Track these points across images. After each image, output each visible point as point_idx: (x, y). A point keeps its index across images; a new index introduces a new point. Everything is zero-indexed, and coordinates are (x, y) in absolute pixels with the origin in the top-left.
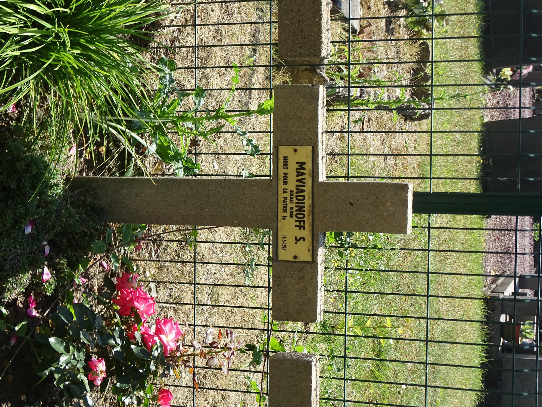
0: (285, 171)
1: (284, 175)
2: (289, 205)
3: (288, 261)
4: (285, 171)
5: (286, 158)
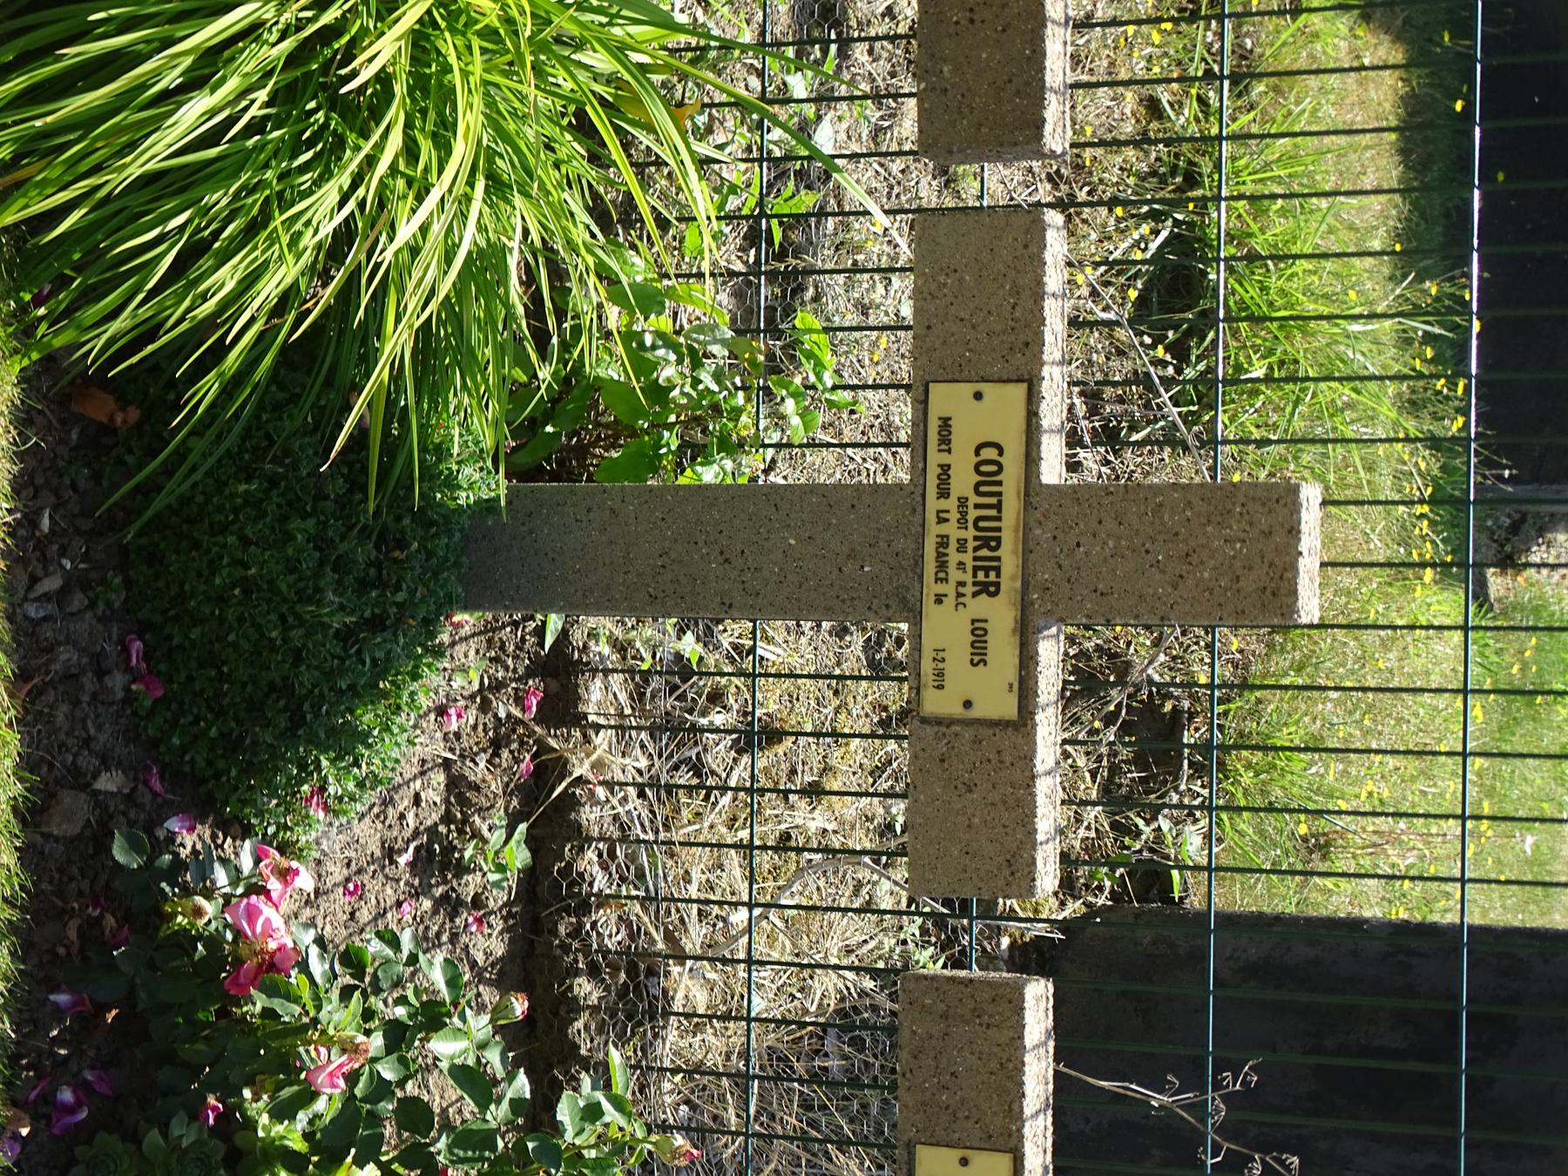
0: (945, 458)
2: (954, 557)
3: (950, 722)
4: (945, 458)
5: (945, 423)
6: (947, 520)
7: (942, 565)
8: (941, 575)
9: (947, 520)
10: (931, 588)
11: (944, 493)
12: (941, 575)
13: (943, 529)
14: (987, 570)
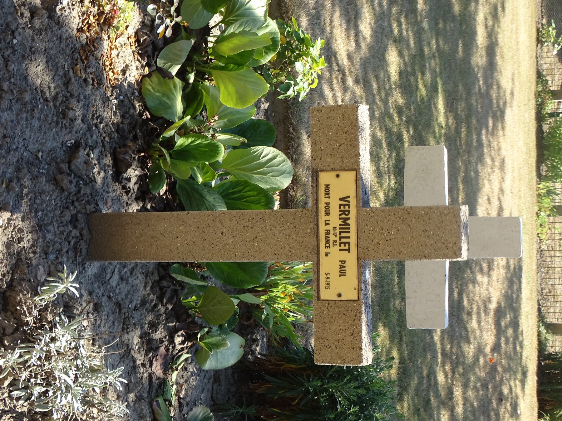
0: (327, 200)
1: (325, 205)
2: (332, 238)
4: (327, 200)
5: (327, 186)
6: (329, 224)
7: (327, 241)
8: (327, 245)
9: (329, 224)
10: (323, 250)
11: (327, 214)
12: (327, 245)
13: (327, 227)
14: (344, 205)
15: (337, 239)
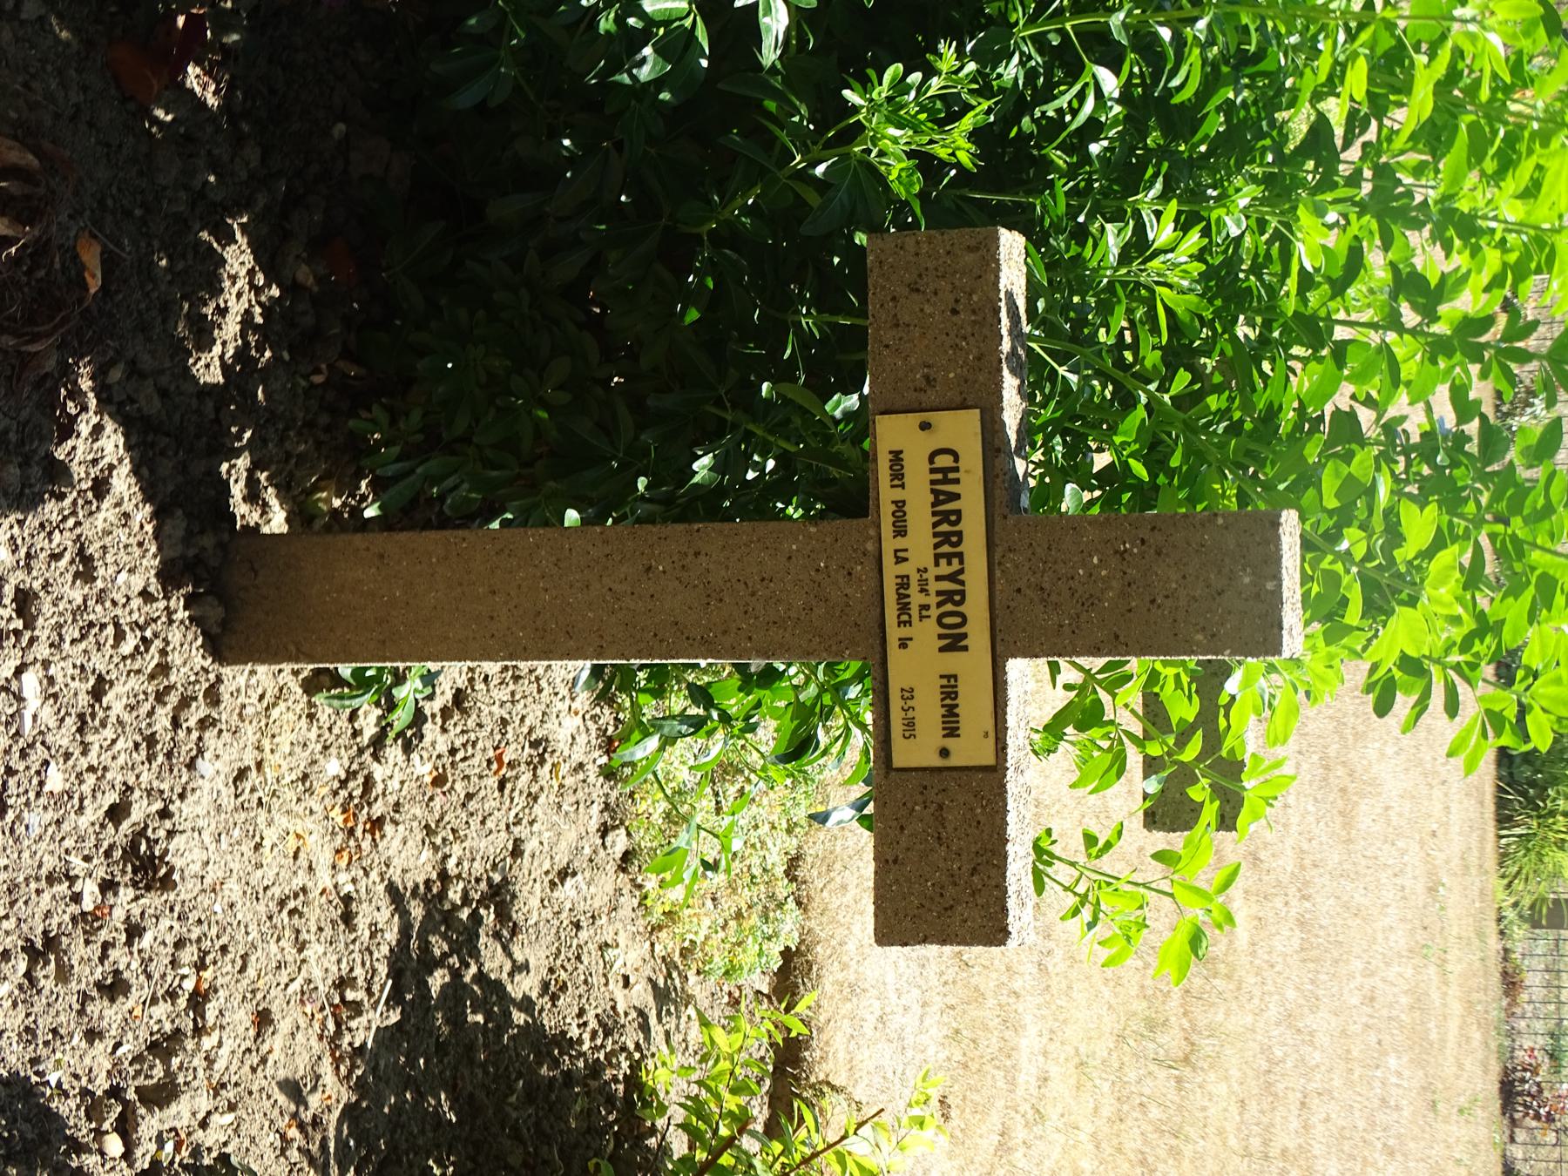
0: (898, 494)
1: (894, 508)
4: (898, 494)
5: (897, 456)
6: (906, 560)
7: (904, 608)
9: (906, 560)
10: (894, 633)
13: (903, 569)
15: (933, 600)
